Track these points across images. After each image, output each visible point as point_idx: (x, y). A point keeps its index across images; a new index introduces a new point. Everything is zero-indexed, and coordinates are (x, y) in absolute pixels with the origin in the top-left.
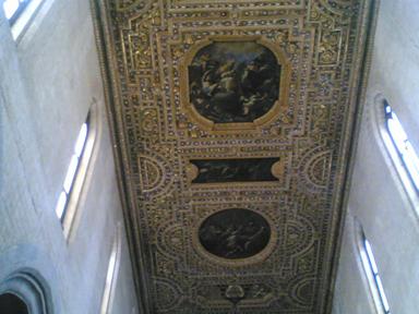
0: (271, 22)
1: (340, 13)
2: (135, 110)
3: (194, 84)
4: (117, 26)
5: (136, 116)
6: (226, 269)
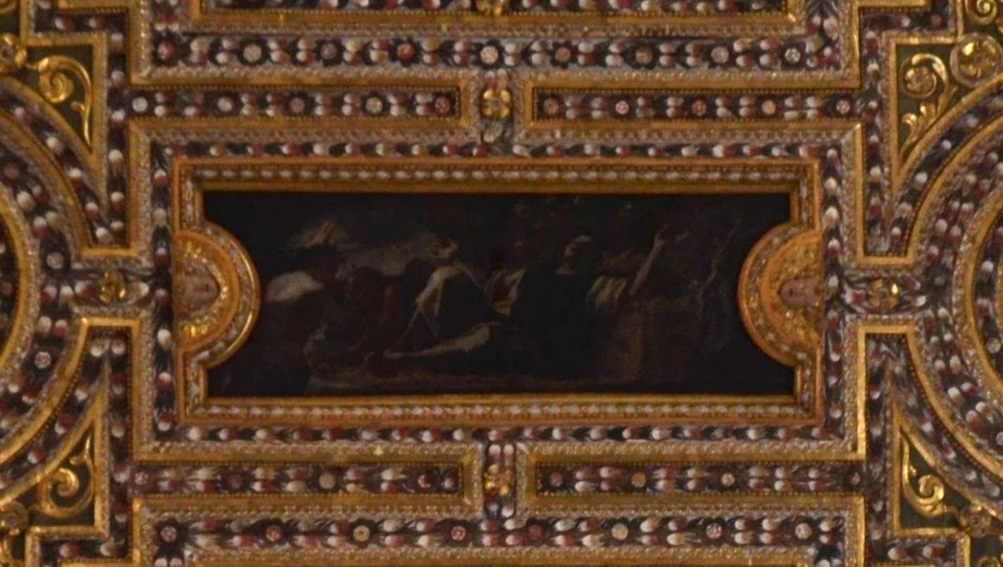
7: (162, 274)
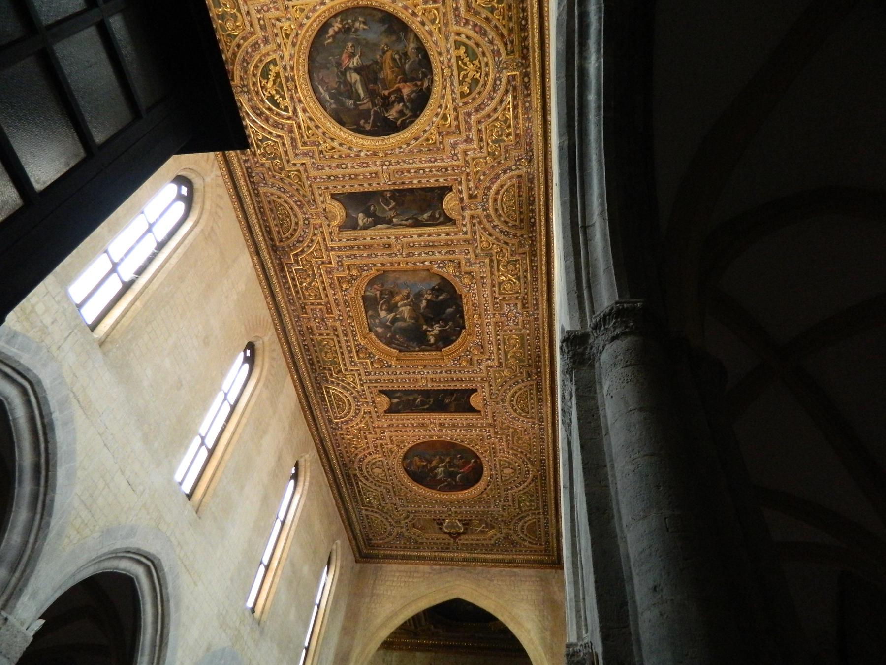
0: (440, 253)
1: (516, 241)
2: (312, 340)
3: (370, 313)
4: (280, 259)
5: (314, 346)
6: (441, 503)
7: (373, 402)
